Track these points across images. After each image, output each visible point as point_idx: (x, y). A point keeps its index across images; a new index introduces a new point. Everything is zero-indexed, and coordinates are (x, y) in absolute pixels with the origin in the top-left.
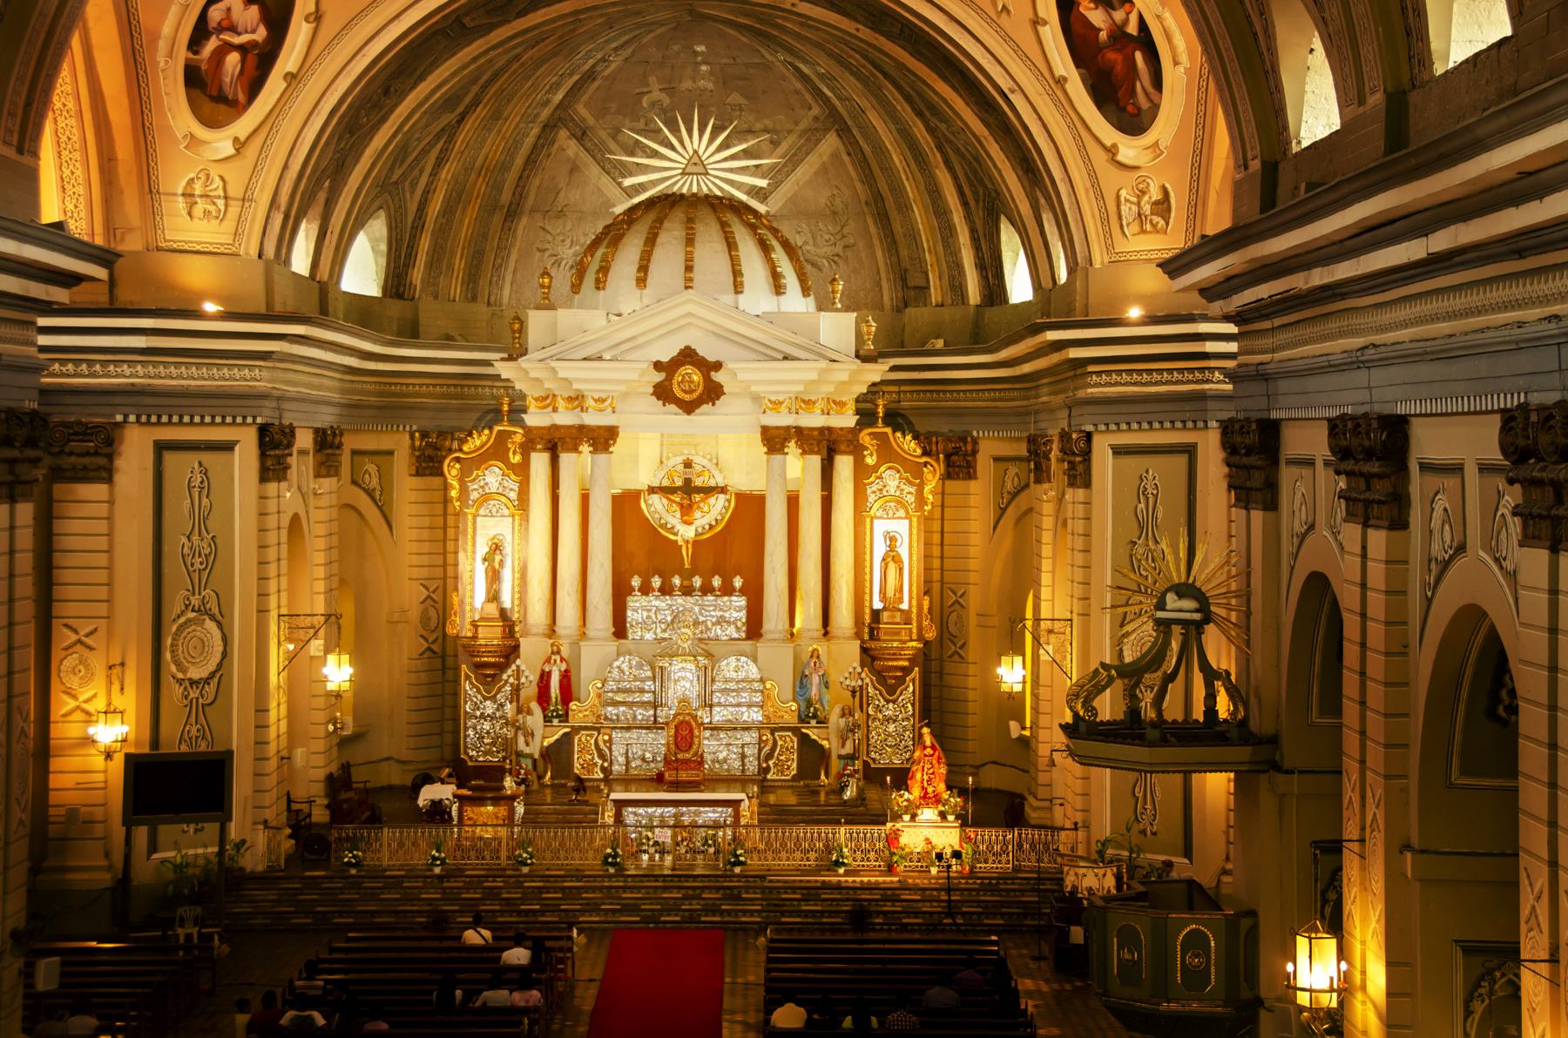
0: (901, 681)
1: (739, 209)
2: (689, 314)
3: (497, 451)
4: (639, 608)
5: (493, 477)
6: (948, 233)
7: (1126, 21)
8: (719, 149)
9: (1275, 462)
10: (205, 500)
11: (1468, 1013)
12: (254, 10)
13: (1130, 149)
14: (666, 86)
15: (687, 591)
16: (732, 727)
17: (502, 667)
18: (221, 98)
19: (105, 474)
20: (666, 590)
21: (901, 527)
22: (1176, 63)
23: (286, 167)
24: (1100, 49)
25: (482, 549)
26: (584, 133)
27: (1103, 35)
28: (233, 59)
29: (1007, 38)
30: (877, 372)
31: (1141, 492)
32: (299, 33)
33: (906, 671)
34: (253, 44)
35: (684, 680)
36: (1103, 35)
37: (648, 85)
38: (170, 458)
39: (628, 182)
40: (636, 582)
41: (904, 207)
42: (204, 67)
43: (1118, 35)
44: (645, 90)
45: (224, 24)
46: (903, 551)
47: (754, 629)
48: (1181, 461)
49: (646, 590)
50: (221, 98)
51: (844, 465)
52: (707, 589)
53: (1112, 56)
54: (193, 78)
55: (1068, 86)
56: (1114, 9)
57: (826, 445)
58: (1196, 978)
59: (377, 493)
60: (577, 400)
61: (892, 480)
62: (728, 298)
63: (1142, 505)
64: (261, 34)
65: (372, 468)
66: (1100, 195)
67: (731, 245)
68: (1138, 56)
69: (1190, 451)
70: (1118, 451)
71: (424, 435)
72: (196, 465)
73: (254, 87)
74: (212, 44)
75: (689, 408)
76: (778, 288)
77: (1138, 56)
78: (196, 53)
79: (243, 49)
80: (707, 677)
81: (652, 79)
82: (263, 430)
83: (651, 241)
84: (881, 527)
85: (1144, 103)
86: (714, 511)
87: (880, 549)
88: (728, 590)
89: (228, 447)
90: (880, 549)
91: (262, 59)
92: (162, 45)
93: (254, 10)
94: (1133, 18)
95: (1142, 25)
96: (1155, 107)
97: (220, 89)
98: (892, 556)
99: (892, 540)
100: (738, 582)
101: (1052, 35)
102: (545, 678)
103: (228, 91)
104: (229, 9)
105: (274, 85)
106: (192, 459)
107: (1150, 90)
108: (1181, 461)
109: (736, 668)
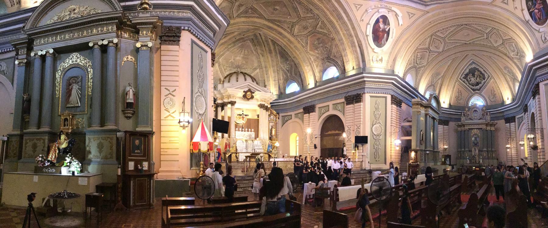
7: (387, 28)
13: (377, 49)
22: (392, 38)
24: (379, 31)
27: (381, 29)
31: (376, 103)
36: (381, 29)
43: (384, 31)
53: (380, 33)
55: (368, 37)
56: (385, 25)
63: (376, 105)
68: (386, 35)
77: (386, 35)
85: (383, 43)
94: (388, 28)
95: (389, 30)
96: (385, 44)
107: (385, 41)
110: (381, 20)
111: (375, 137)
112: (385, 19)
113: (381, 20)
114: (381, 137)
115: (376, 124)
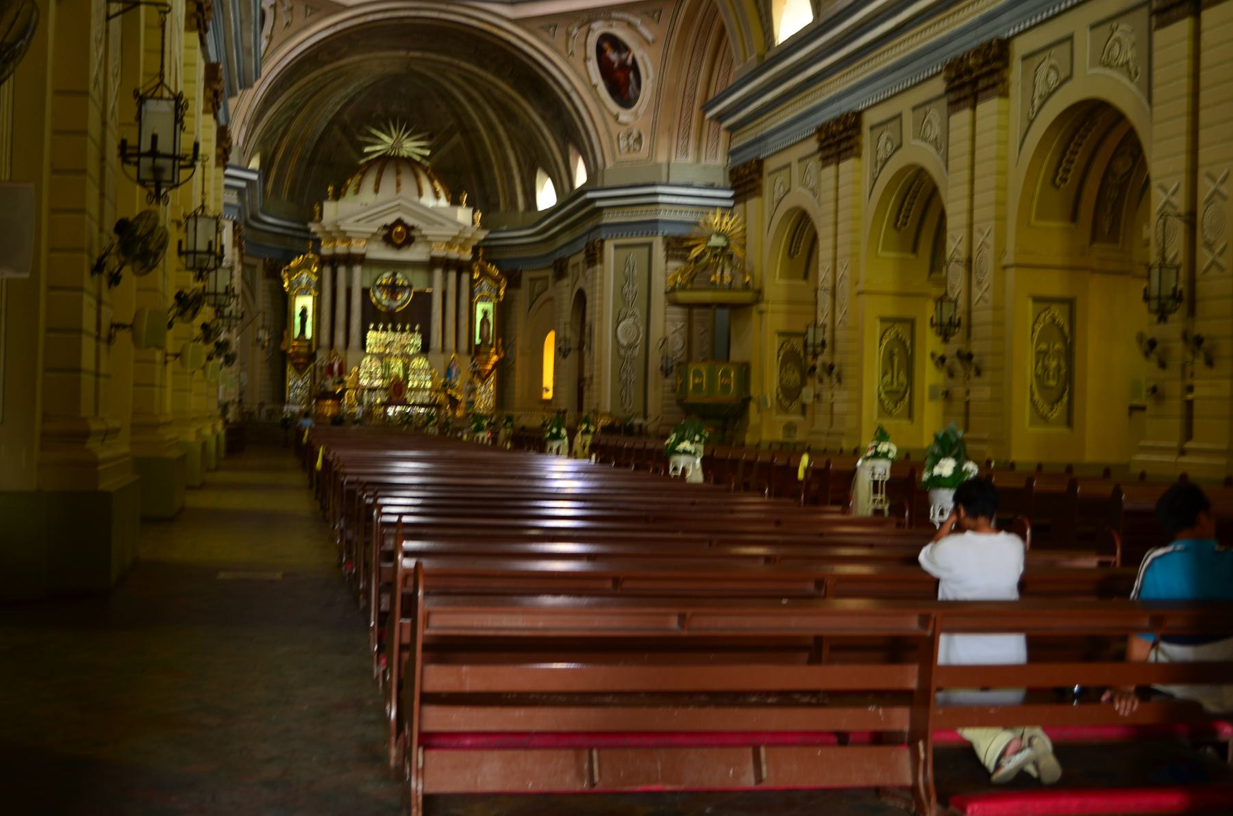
0: (488, 375)
1: (418, 163)
2: (399, 205)
3: (306, 266)
4: (372, 336)
5: (305, 277)
6: (510, 179)
7: (627, 58)
8: (408, 137)
9: (761, 175)
11: (880, 345)
13: (625, 116)
15: (394, 330)
16: (417, 389)
17: (306, 365)
20: (385, 329)
21: (489, 306)
22: (647, 77)
23: (249, 106)
25: (298, 311)
27: (616, 65)
29: (572, 67)
30: (482, 235)
31: (627, 263)
33: (491, 371)
35: (397, 367)
36: (616, 65)
39: (367, 149)
40: (372, 326)
41: (490, 168)
43: (623, 64)
46: (490, 317)
47: (425, 349)
48: (646, 250)
49: (376, 329)
51: (465, 277)
52: (403, 330)
53: (620, 75)
55: (598, 88)
57: (459, 267)
58: (726, 387)
59: (250, 283)
60: (347, 239)
61: (485, 284)
62: (416, 199)
66: (610, 136)
67: (417, 177)
68: (631, 75)
69: (650, 246)
70: (616, 247)
71: (270, 260)
75: (399, 247)
76: (437, 196)
77: (631, 75)
80: (406, 368)
82: (235, 224)
83: (380, 173)
84: (480, 307)
86: (404, 298)
87: (479, 316)
88: (412, 330)
90: (479, 316)
95: (634, 60)
96: (637, 98)
98: (484, 320)
99: (485, 313)
100: (417, 327)
101: (593, 66)
102: (331, 366)
108: (646, 250)
109: (419, 363)
110: (606, 45)
111: (622, 352)
112: (609, 41)
113: (606, 45)
114: (637, 351)
115: (624, 319)
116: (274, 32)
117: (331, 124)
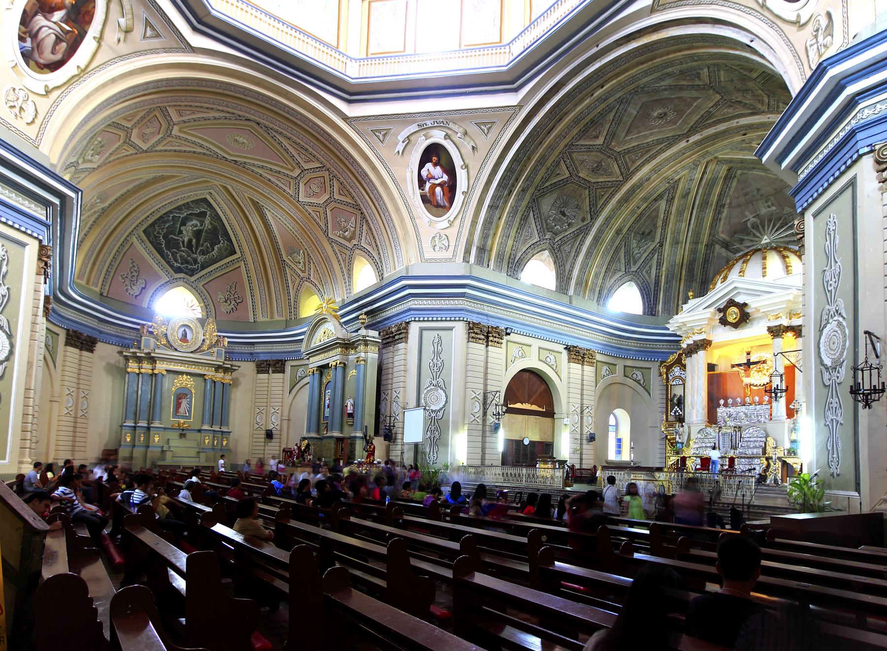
10: (439, 347)
12: (438, 167)
14: (755, 215)
18: (438, 206)
19: (405, 339)
26: (727, 245)
28: (438, 190)
32: (461, 175)
34: (445, 182)
37: (747, 217)
38: (425, 333)
42: (428, 195)
44: (747, 219)
45: (429, 176)
50: (438, 206)
54: (425, 199)
64: (445, 178)
65: (639, 373)
72: (436, 336)
73: (451, 200)
74: (428, 185)
78: (423, 190)
79: (439, 185)
81: (747, 213)
89: (451, 329)
91: (451, 188)
92: (410, 188)
93: (438, 167)
97: (437, 201)
103: (441, 203)
104: (428, 170)
105: (459, 198)
106: (435, 333)
116: (467, 162)
117: (710, 246)
